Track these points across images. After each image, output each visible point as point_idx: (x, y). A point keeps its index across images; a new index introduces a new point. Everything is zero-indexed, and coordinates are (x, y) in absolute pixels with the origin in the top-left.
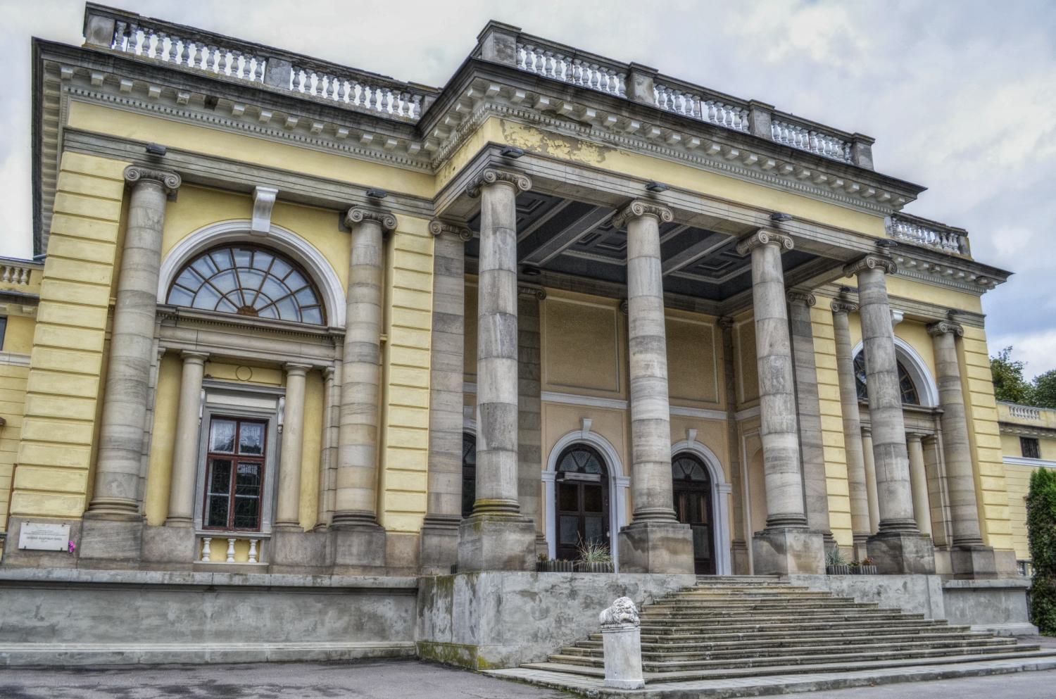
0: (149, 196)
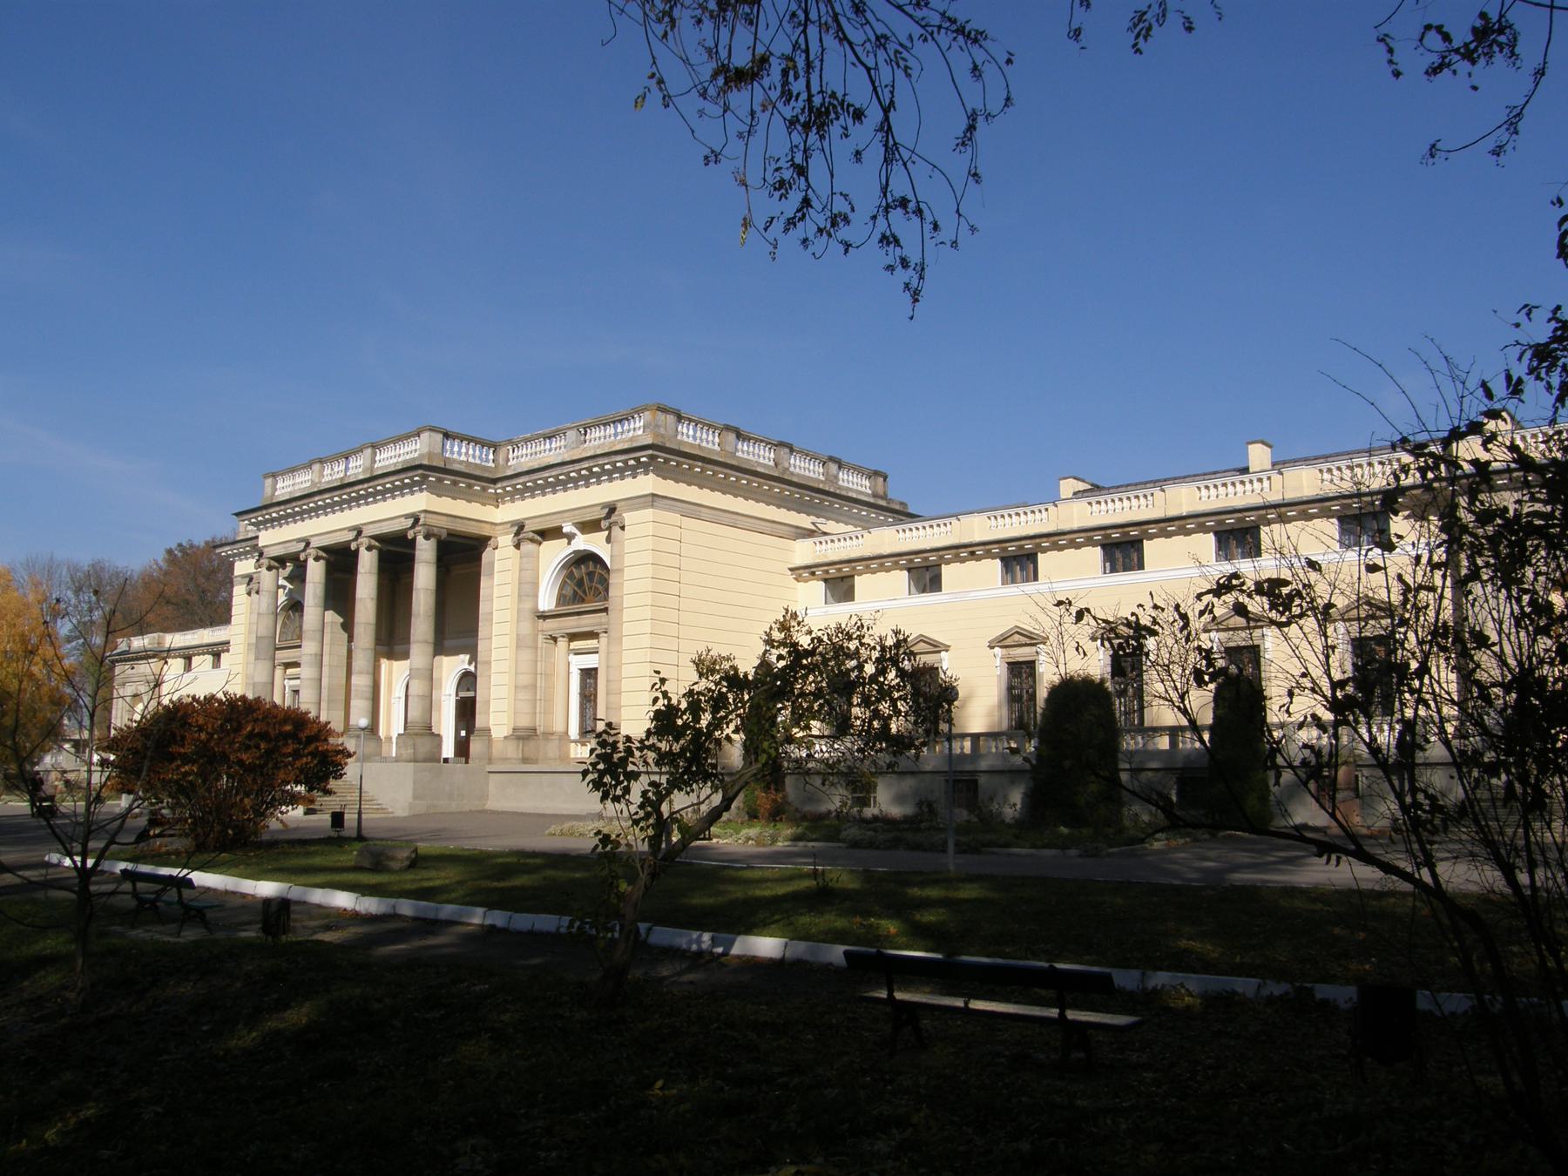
0: (254, 595)
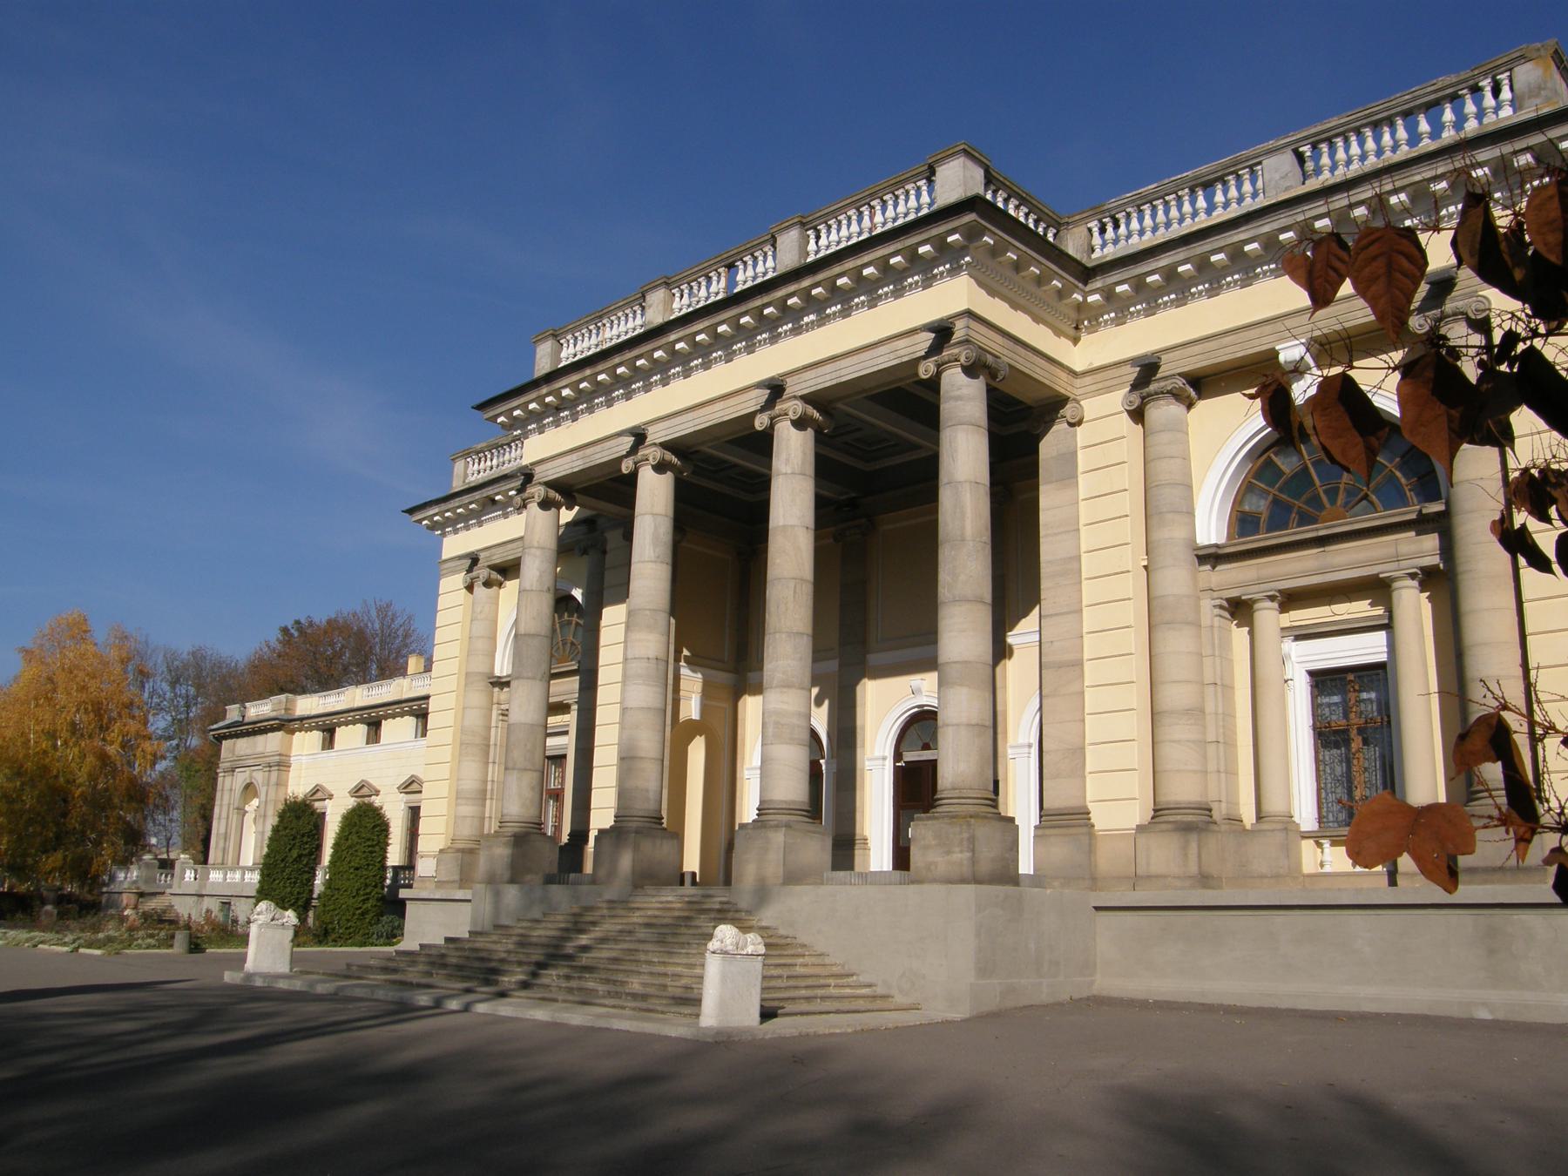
0: (479, 590)
